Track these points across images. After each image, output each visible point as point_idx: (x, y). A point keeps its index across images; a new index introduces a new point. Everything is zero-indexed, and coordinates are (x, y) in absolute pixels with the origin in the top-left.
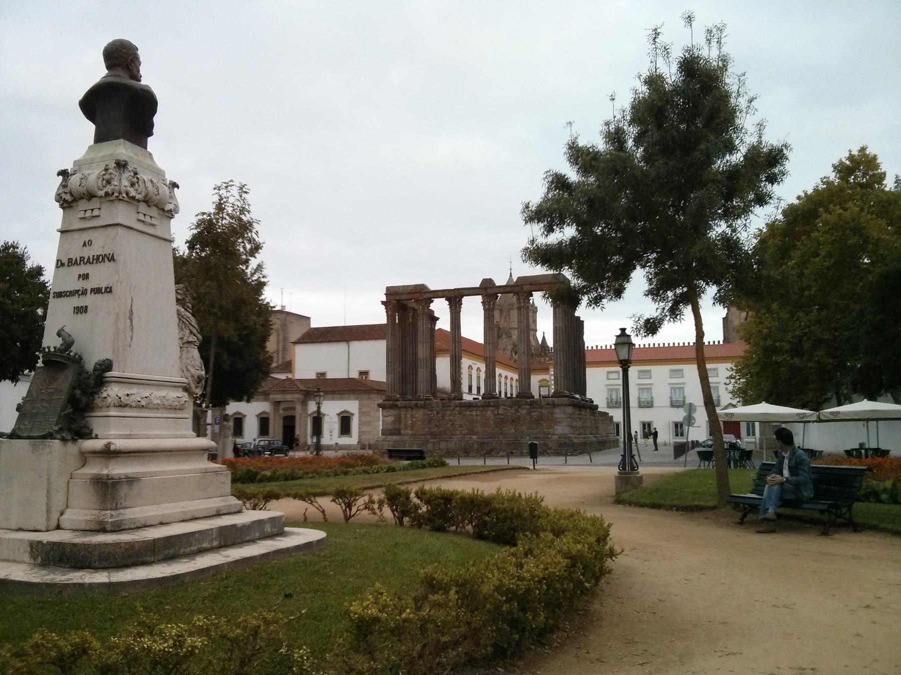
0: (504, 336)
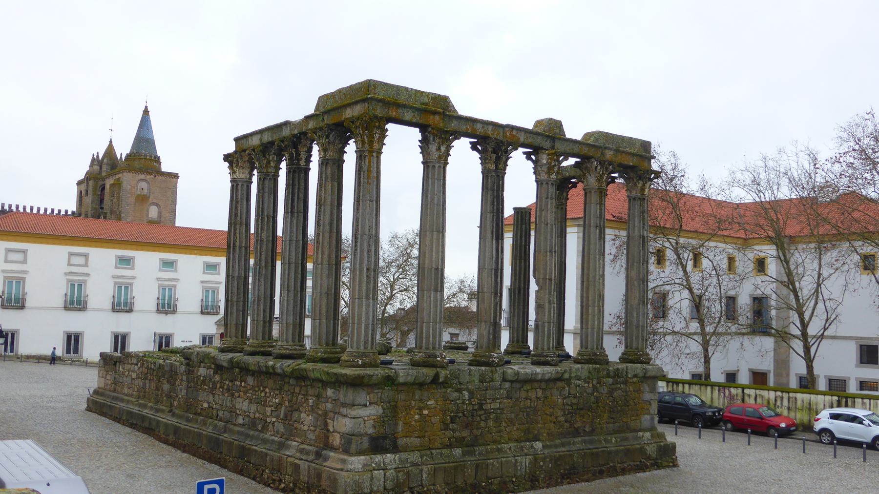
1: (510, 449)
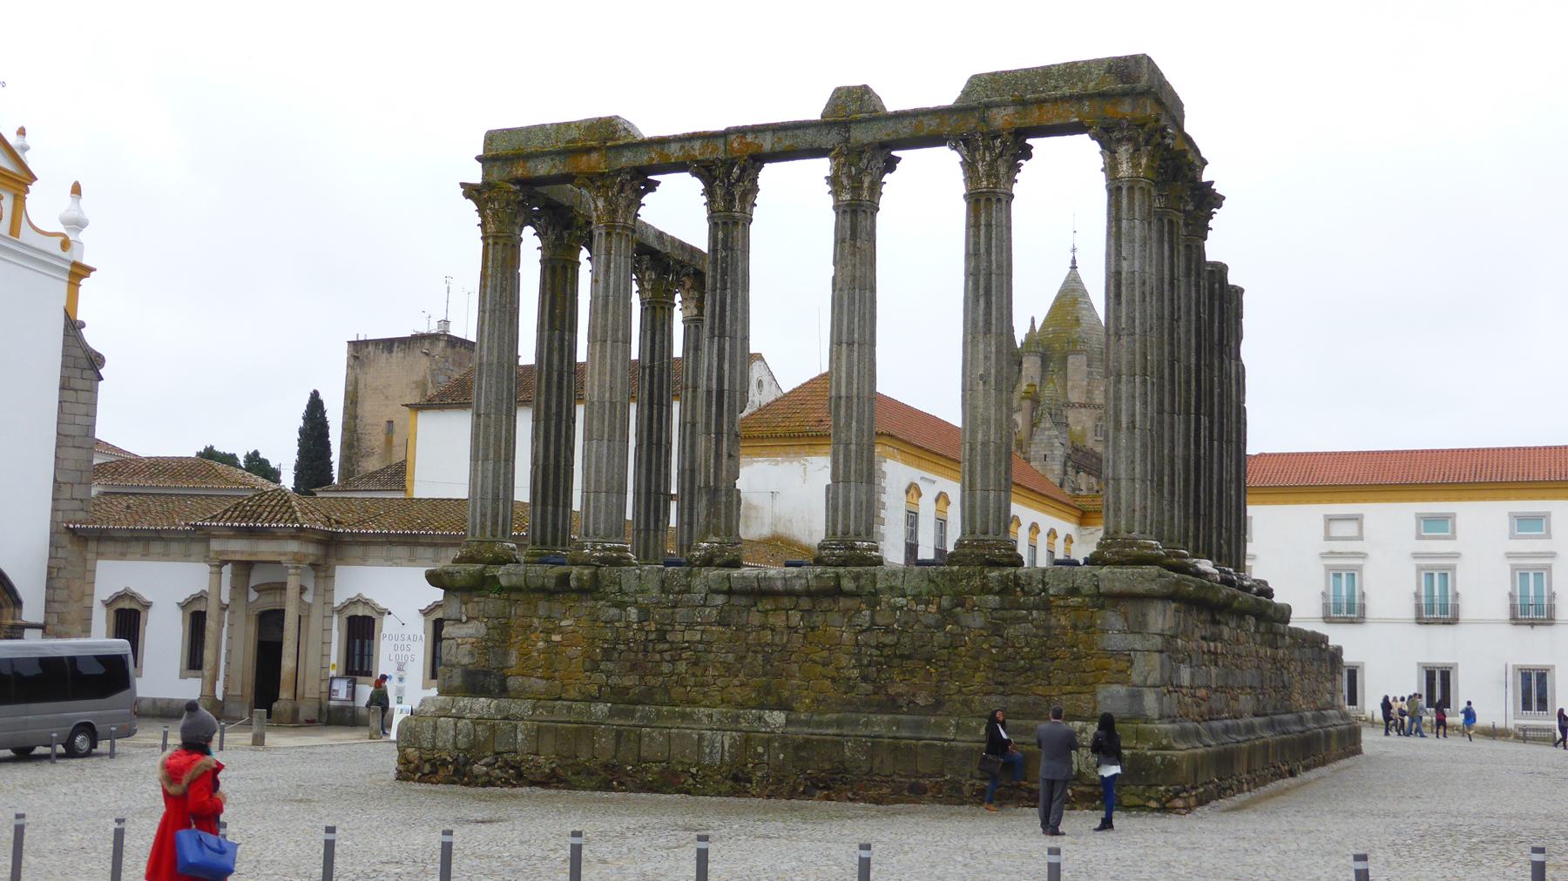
0: (1046, 423)
1: (710, 716)
